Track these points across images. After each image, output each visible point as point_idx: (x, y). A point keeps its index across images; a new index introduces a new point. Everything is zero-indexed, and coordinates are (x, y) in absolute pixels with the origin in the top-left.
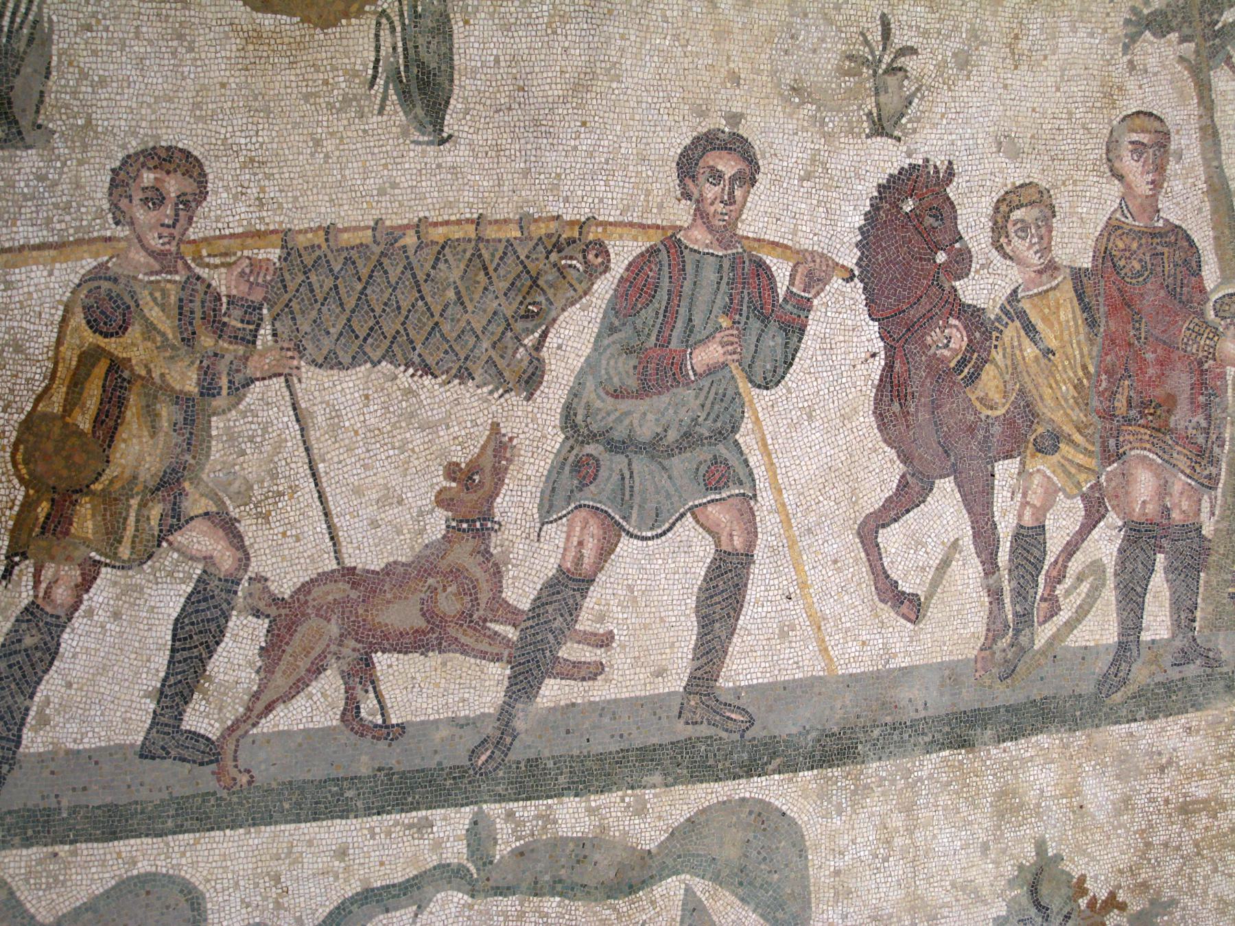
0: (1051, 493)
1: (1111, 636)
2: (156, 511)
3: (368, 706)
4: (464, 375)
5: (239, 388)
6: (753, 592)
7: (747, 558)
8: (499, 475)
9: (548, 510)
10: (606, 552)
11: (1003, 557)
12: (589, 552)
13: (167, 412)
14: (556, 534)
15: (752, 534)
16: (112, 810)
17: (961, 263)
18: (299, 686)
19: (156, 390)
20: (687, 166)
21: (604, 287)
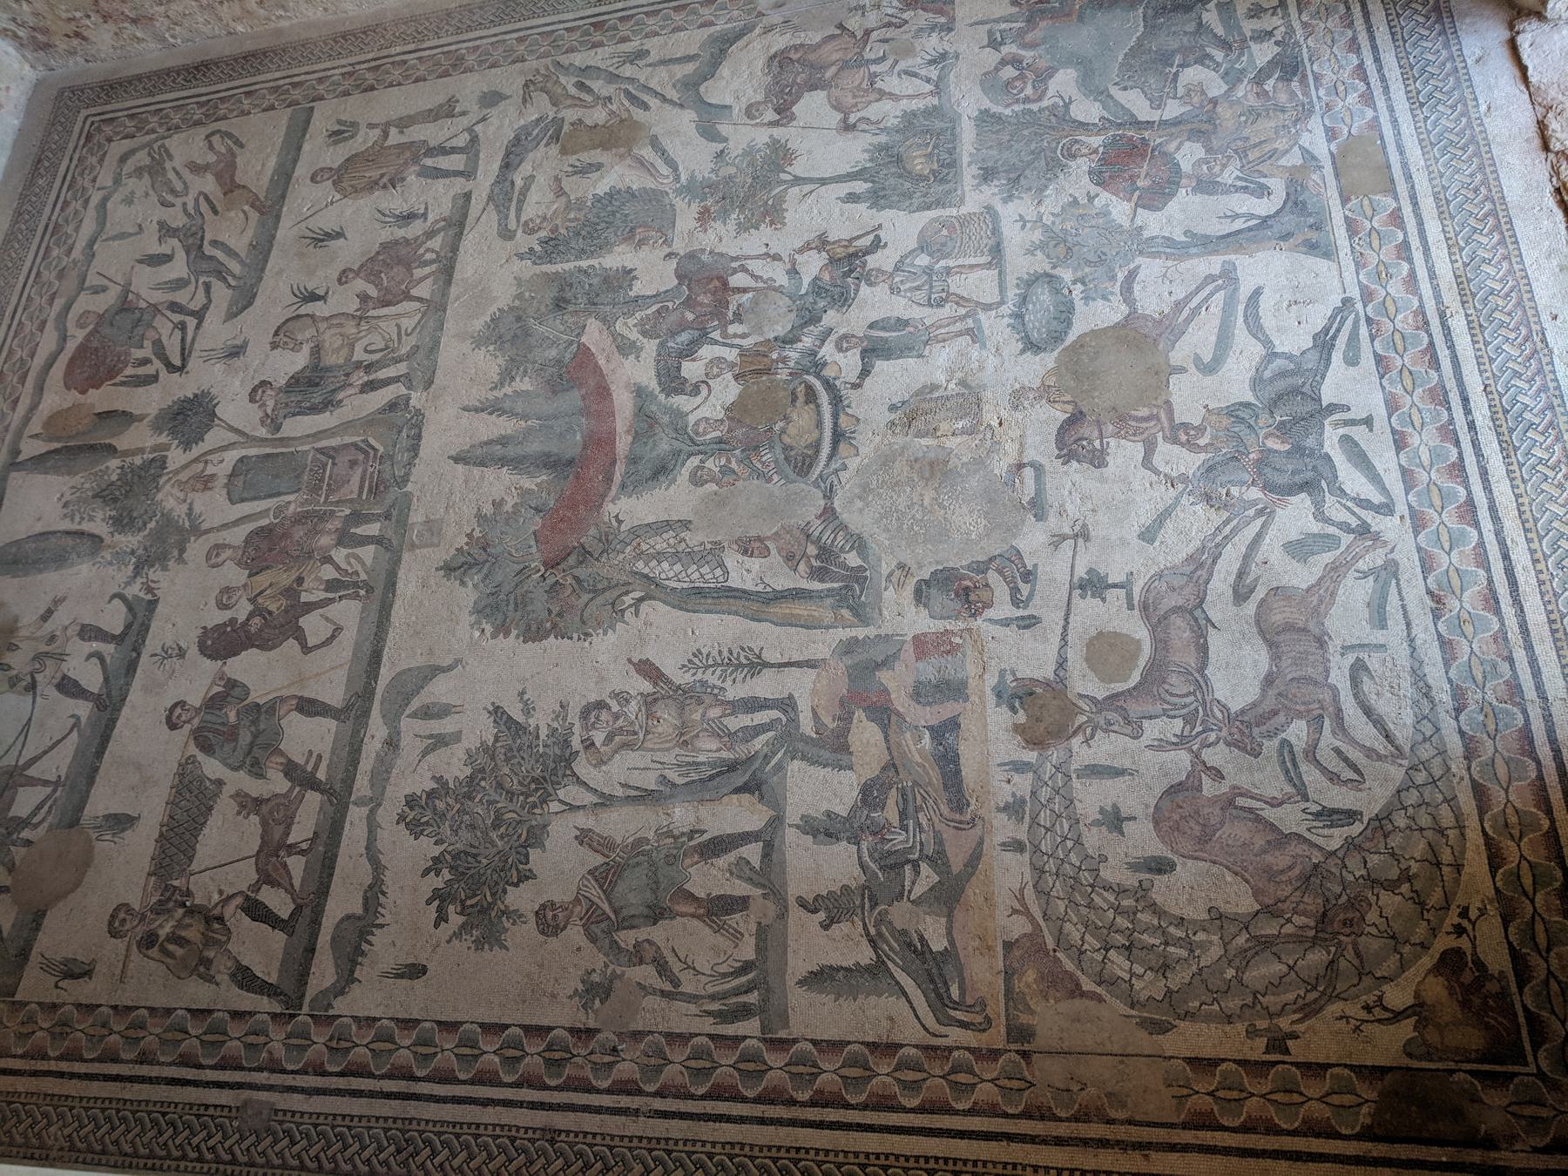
0: (318, 579)
1: (372, 548)
2: (217, 926)
3: (304, 846)
4: (210, 809)
5: (189, 893)
6: (313, 696)
7: (301, 698)
8: (247, 795)
9: (260, 775)
10: (282, 754)
11: (330, 595)
12: (283, 760)
13: (187, 921)
14: (271, 773)
15: (295, 697)
16: (306, 950)
17: (233, 621)
18: (288, 873)
19: (179, 925)
20: (173, 726)
21: (201, 757)
